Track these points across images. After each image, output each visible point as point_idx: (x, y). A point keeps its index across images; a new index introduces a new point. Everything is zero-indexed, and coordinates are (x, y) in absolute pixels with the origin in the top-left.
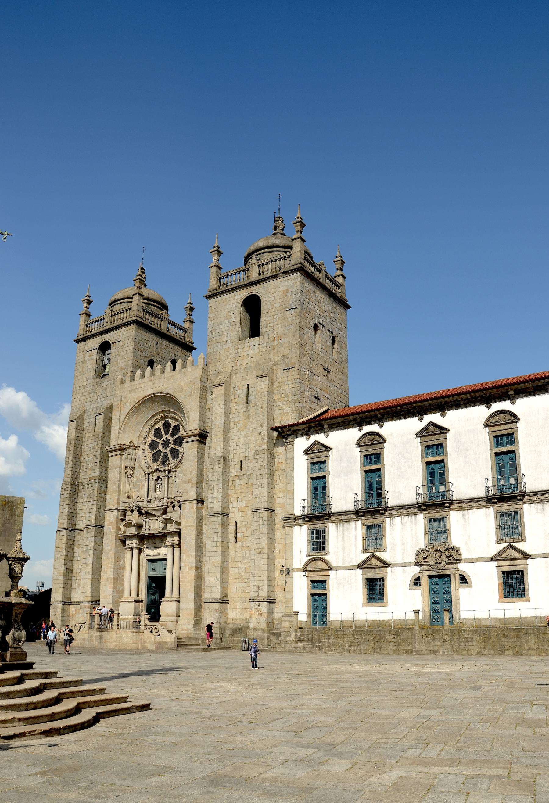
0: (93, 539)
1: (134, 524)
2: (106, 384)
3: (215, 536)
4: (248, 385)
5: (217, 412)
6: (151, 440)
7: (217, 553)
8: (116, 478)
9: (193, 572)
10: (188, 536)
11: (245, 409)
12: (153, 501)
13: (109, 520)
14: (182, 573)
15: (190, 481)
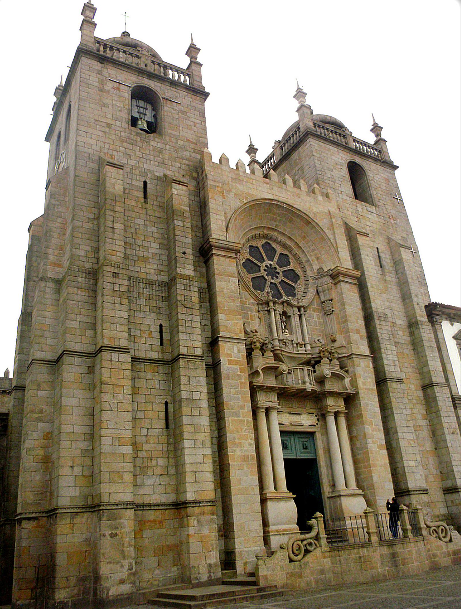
0: (203, 381)
1: (284, 370)
2: (160, 145)
3: (403, 407)
4: (377, 248)
5: (367, 262)
6: (246, 258)
7: (410, 428)
8: (233, 292)
9: (385, 452)
10: (370, 402)
11: (380, 272)
12: (287, 344)
13: (230, 356)
14: (372, 453)
15: (358, 332)
